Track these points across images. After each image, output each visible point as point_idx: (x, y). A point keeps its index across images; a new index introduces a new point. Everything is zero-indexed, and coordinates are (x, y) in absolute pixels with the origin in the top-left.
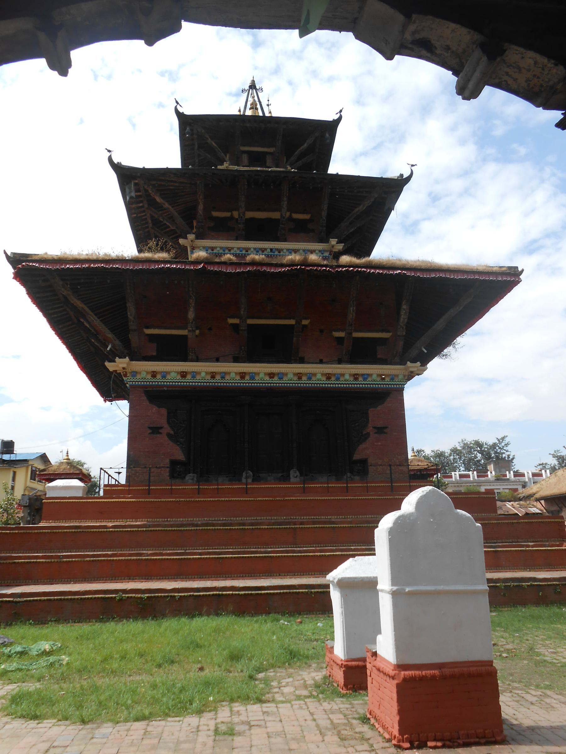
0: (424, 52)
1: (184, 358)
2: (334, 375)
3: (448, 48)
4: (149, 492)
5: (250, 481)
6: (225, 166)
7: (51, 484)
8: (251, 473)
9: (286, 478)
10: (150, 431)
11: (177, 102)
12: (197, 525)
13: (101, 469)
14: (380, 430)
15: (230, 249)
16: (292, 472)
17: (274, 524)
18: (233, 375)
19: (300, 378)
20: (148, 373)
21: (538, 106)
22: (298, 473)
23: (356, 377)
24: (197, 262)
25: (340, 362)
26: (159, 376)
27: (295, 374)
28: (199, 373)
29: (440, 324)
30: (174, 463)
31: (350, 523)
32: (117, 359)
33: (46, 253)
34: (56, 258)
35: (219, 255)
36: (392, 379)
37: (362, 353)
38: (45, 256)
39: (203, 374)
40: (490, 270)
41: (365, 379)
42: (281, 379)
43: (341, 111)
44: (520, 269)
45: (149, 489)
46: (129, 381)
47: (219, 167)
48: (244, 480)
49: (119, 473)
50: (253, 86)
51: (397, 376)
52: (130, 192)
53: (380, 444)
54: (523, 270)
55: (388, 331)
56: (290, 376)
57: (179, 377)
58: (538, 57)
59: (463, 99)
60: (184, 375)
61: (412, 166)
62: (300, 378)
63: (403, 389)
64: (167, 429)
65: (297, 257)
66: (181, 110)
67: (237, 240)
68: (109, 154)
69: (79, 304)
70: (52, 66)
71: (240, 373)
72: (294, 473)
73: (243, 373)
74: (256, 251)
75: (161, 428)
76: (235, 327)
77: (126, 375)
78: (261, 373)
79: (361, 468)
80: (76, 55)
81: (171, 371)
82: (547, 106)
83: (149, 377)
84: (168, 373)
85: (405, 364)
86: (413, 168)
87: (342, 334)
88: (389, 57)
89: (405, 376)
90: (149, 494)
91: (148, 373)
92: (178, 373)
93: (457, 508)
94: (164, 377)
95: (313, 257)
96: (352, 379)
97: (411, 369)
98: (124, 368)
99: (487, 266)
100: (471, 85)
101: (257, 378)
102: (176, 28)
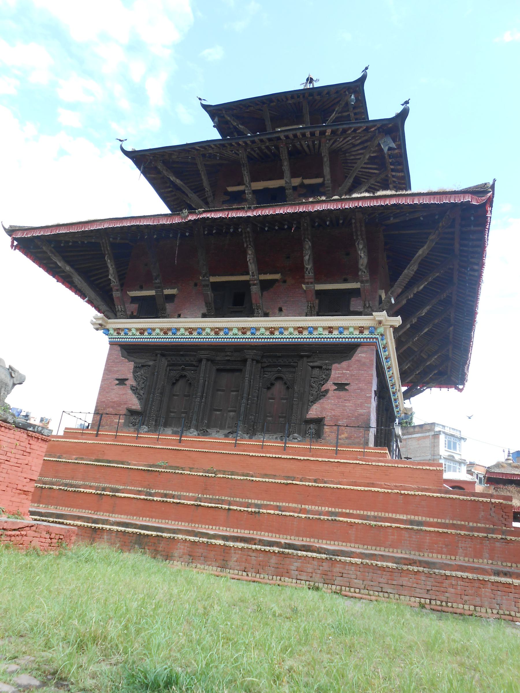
10: (117, 382)
30: (132, 412)
64: (131, 382)
75: (128, 379)
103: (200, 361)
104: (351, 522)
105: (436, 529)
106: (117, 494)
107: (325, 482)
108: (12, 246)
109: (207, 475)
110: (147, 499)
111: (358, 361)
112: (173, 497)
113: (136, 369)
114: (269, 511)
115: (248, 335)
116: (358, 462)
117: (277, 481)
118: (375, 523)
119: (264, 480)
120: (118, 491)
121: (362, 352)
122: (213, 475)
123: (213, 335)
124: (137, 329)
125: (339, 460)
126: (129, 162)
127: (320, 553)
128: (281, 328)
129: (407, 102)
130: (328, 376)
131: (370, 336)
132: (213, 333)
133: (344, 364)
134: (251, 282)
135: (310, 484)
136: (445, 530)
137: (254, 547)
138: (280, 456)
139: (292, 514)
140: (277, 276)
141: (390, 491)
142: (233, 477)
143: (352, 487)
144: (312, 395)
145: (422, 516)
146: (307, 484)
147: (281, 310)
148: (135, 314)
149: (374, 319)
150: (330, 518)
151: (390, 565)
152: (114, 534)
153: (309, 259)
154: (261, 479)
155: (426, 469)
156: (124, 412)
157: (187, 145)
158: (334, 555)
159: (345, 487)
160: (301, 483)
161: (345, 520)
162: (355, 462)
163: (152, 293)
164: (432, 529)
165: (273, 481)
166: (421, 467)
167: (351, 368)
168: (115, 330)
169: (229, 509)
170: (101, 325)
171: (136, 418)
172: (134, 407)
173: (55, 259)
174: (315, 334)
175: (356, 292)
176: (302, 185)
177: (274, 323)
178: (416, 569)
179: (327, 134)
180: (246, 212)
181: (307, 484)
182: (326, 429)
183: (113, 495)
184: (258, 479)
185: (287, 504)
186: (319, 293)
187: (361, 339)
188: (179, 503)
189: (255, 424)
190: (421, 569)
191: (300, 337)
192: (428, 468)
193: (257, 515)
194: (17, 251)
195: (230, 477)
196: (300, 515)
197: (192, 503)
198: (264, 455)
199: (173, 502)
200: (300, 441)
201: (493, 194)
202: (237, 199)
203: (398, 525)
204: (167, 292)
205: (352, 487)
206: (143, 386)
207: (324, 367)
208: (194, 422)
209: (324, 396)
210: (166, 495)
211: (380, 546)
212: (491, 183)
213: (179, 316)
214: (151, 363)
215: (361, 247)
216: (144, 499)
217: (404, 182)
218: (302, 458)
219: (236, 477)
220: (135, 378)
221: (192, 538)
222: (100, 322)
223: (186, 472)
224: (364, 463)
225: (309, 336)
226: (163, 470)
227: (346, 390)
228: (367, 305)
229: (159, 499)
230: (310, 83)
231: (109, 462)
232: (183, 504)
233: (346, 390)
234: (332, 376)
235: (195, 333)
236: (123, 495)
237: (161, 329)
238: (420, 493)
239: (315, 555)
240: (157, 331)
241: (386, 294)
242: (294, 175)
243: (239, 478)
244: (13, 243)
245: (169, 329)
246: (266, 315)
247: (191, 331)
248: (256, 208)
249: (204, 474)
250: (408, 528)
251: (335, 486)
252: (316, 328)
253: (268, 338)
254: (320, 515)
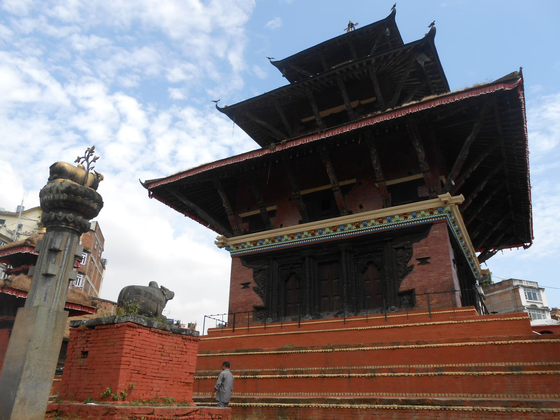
10: (242, 286)
30: (258, 309)
64: (253, 284)
75: (250, 283)
103: (304, 259)
104: (456, 375)
105: (535, 372)
106: (257, 376)
107: (426, 343)
108: (150, 195)
109: (326, 350)
110: (281, 377)
111: (433, 237)
112: (302, 372)
113: (255, 273)
114: (383, 374)
115: (339, 231)
116: (450, 322)
117: (384, 348)
118: (477, 373)
119: (374, 348)
120: (257, 373)
121: (435, 230)
122: (331, 350)
123: (310, 236)
124: (251, 242)
125: (434, 323)
127: (434, 405)
128: (364, 221)
129: (433, 24)
130: (411, 254)
131: (440, 215)
132: (310, 235)
133: (423, 242)
134: (333, 189)
135: (413, 346)
136: (544, 372)
137: (376, 406)
138: (383, 326)
139: (402, 374)
140: (353, 181)
141: (484, 343)
142: (348, 349)
143: (450, 344)
144: (400, 272)
145: (519, 362)
146: (410, 346)
147: (361, 207)
148: (247, 230)
149: (440, 201)
150: (436, 373)
151: (499, 408)
152: (260, 409)
153: (377, 163)
154: (371, 348)
155: (513, 320)
156: (252, 309)
157: (265, 94)
158: (447, 406)
159: (444, 345)
160: (405, 347)
161: (450, 373)
162: (448, 322)
163: (258, 212)
164: (531, 372)
165: (382, 348)
166: (508, 319)
167: (429, 244)
168: (234, 245)
169: (349, 377)
170: (222, 243)
171: (262, 313)
172: (258, 304)
173: (181, 199)
174: (393, 221)
175: (420, 182)
176: (360, 106)
177: (358, 218)
178: (524, 410)
179: (372, 62)
180: (320, 135)
181: (410, 346)
182: (418, 298)
183: (254, 378)
184: (368, 348)
185: (397, 366)
186: (390, 188)
187: (432, 218)
188: (308, 377)
189: (357, 303)
190: (529, 409)
191: (381, 225)
192: (515, 318)
193: (373, 379)
194: (153, 198)
195: (345, 349)
196: (410, 374)
197: (318, 375)
198: (370, 328)
199: (303, 377)
200: (397, 312)
201: (522, 79)
202: (310, 128)
203: (499, 372)
204: (269, 209)
205: (450, 344)
206: (263, 286)
207: (406, 247)
208: (308, 309)
209: (411, 271)
210: (296, 372)
211: (487, 393)
212: (518, 71)
213: (281, 226)
214: (266, 267)
215: (417, 144)
216: (279, 378)
217: (443, 85)
218: (402, 325)
219: (350, 349)
220: (256, 281)
221: (323, 405)
222: (222, 241)
223: (309, 351)
224: (456, 322)
225: (389, 224)
226: (290, 352)
227: (429, 263)
228: (432, 190)
229: (291, 376)
230: (351, 27)
231: (247, 351)
232: (311, 377)
233: (429, 263)
234: (414, 253)
235: (296, 237)
236: (262, 376)
237: (269, 239)
238: (513, 342)
239: (430, 407)
240: (267, 241)
241: (446, 178)
242: (352, 100)
243: (353, 349)
244: (149, 193)
245: (276, 238)
246: (350, 213)
247: (292, 236)
248: (327, 131)
249: (324, 350)
250: (509, 374)
251: (435, 345)
252: (393, 217)
253: (355, 231)
254: (427, 372)
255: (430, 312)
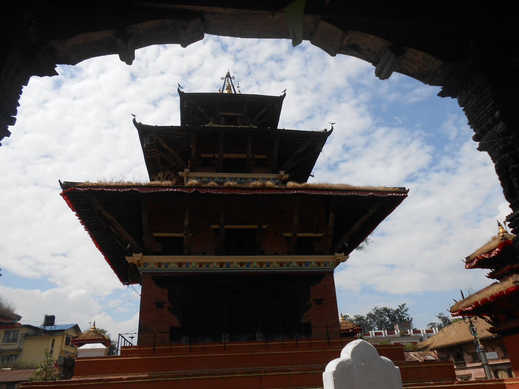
0: (355, 52)
1: (181, 253)
2: (285, 263)
3: (369, 50)
4: (154, 351)
5: (227, 341)
6: (210, 124)
7: (81, 348)
8: (227, 335)
9: (253, 339)
11: (179, 85)
12: (189, 376)
13: (120, 334)
14: (319, 302)
15: (213, 179)
16: (257, 334)
17: (245, 373)
18: (215, 264)
19: (261, 266)
20: (155, 264)
21: (426, 83)
22: (261, 335)
23: (300, 264)
24: (191, 187)
25: (289, 254)
26: (163, 266)
27: (258, 263)
28: (191, 263)
29: (356, 227)
30: (173, 329)
31: (301, 370)
32: (134, 254)
33: (88, 182)
34: (94, 185)
35: (207, 183)
36: (325, 265)
37: (304, 247)
38: (87, 184)
39: (194, 264)
40: (387, 190)
41: (306, 266)
42: (248, 266)
43: (285, 91)
44: (407, 189)
45: (154, 349)
46: (142, 270)
47: (206, 125)
48: (223, 341)
49: (132, 338)
50: (228, 76)
51: (329, 263)
52: (146, 142)
53: (319, 311)
54: (409, 190)
55: (321, 232)
56: (255, 264)
57: (177, 266)
58: (425, 54)
59: (381, 79)
60: (180, 264)
61: (333, 124)
62: (261, 266)
63: (333, 272)
65: (258, 183)
66: (182, 90)
67: (217, 172)
68: (134, 117)
69: (109, 216)
70: (122, 59)
71: (220, 263)
72: (259, 335)
73: (221, 263)
74: (231, 180)
75: (164, 303)
76: (216, 230)
77: (139, 266)
78: (235, 262)
79: (306, 330)
80: (138, 52)
81: (171, 262)
82: (432, 83)
83: (156, 266)
84: (170, 263)
85: (333, 254)
86: (333, 125)
87: (289, 235)
88: (333, 55)
89: (334, 263)
90: (154, 353)
91: (155, 264)
92: (176, 263)
93: (381, 355)
94: (166, 266)
95: (269, 183)
96: (298, 265)
97: (338, 258)
98: (138, 261)
99: (385, 187)
100: (385, 71)
101: (231, 266)
102: (201, 37)
126: (135, 132)
255: (328, 339)
